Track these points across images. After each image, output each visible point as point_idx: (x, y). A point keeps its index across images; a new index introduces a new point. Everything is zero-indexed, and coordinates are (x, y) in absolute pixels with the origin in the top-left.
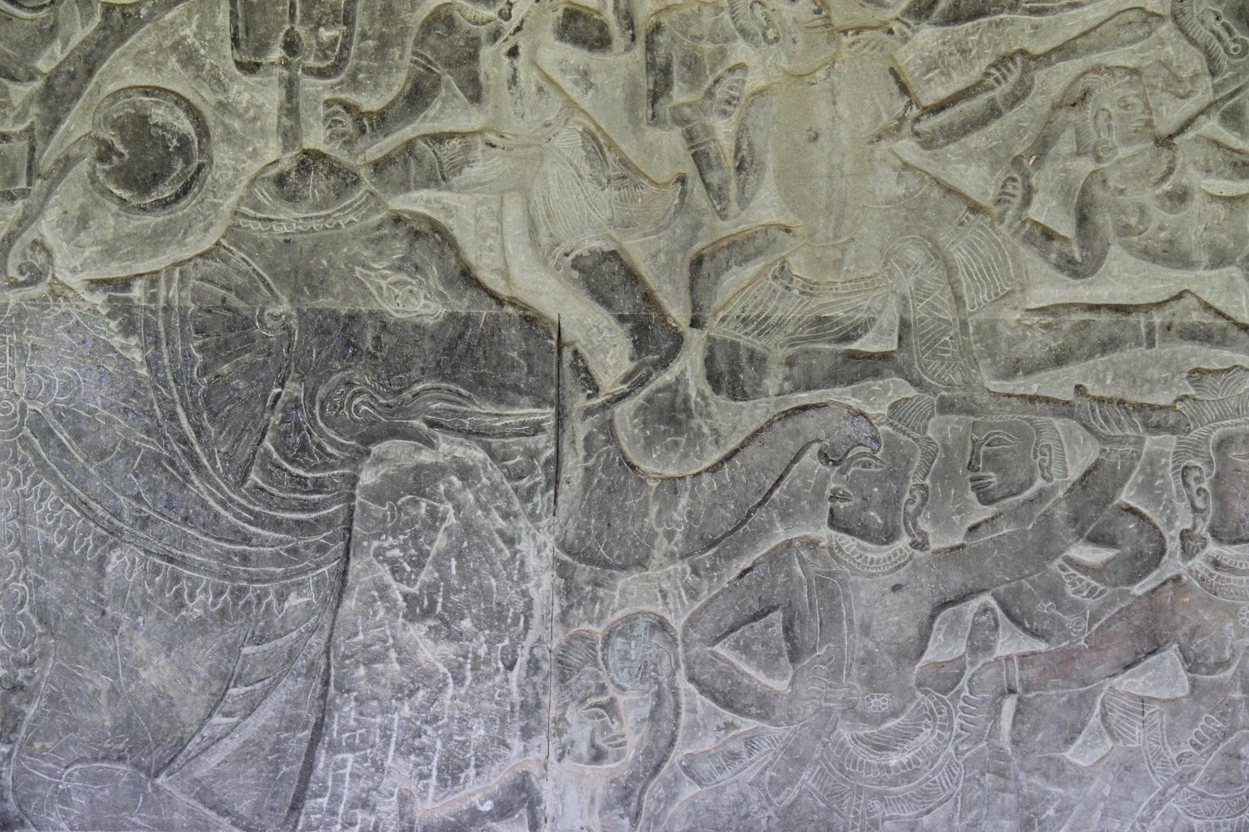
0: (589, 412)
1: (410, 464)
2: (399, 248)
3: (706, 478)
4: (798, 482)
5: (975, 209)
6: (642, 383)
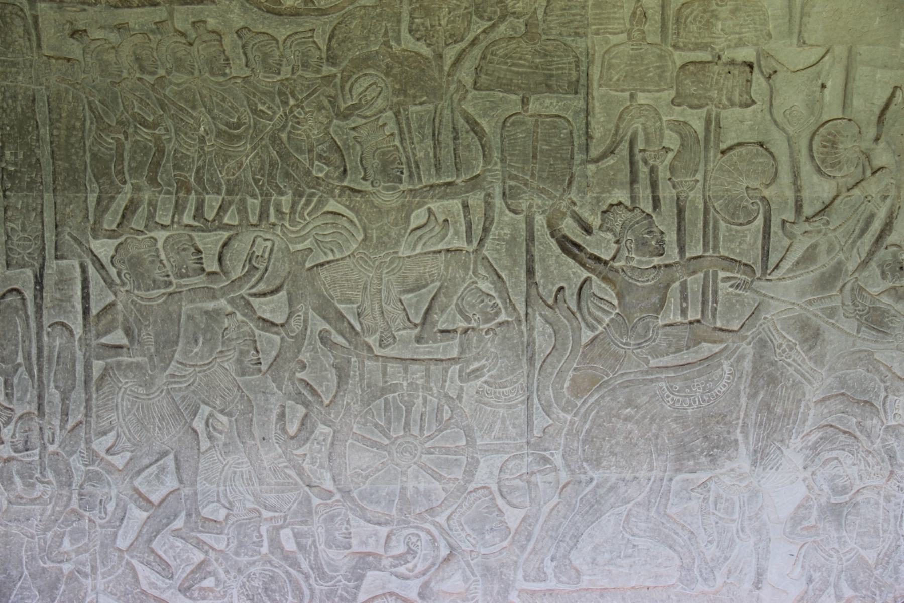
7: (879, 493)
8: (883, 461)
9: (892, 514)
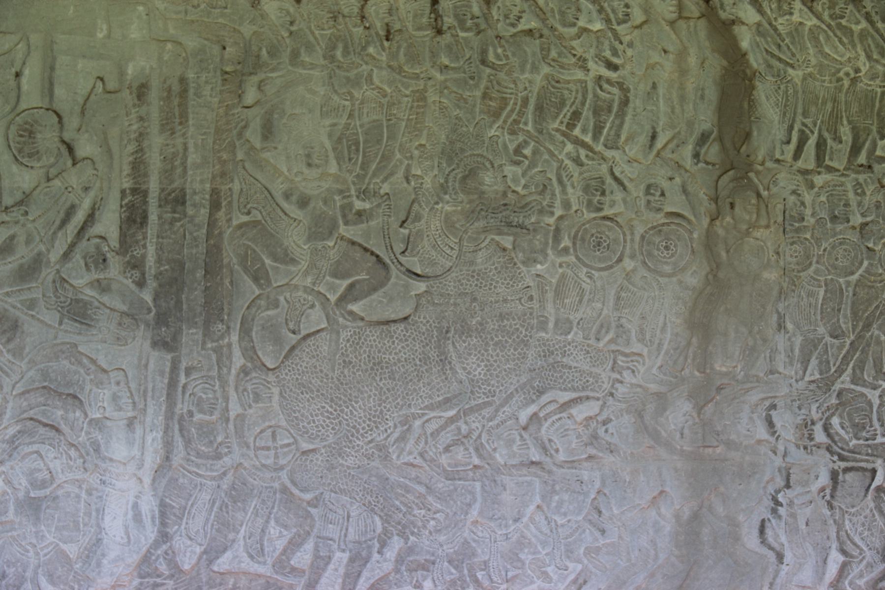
7: (80, 487)
8: (88, 454)
9: (93, 507)
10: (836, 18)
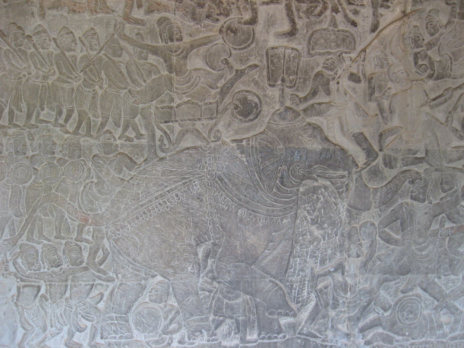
0: (357, 172)
1: (312, 186)
2: (310, 131)
3: (384, 188)
4: (404, 189)
5: (442, 124)
6: (369, 165)
10: (18, 46)
